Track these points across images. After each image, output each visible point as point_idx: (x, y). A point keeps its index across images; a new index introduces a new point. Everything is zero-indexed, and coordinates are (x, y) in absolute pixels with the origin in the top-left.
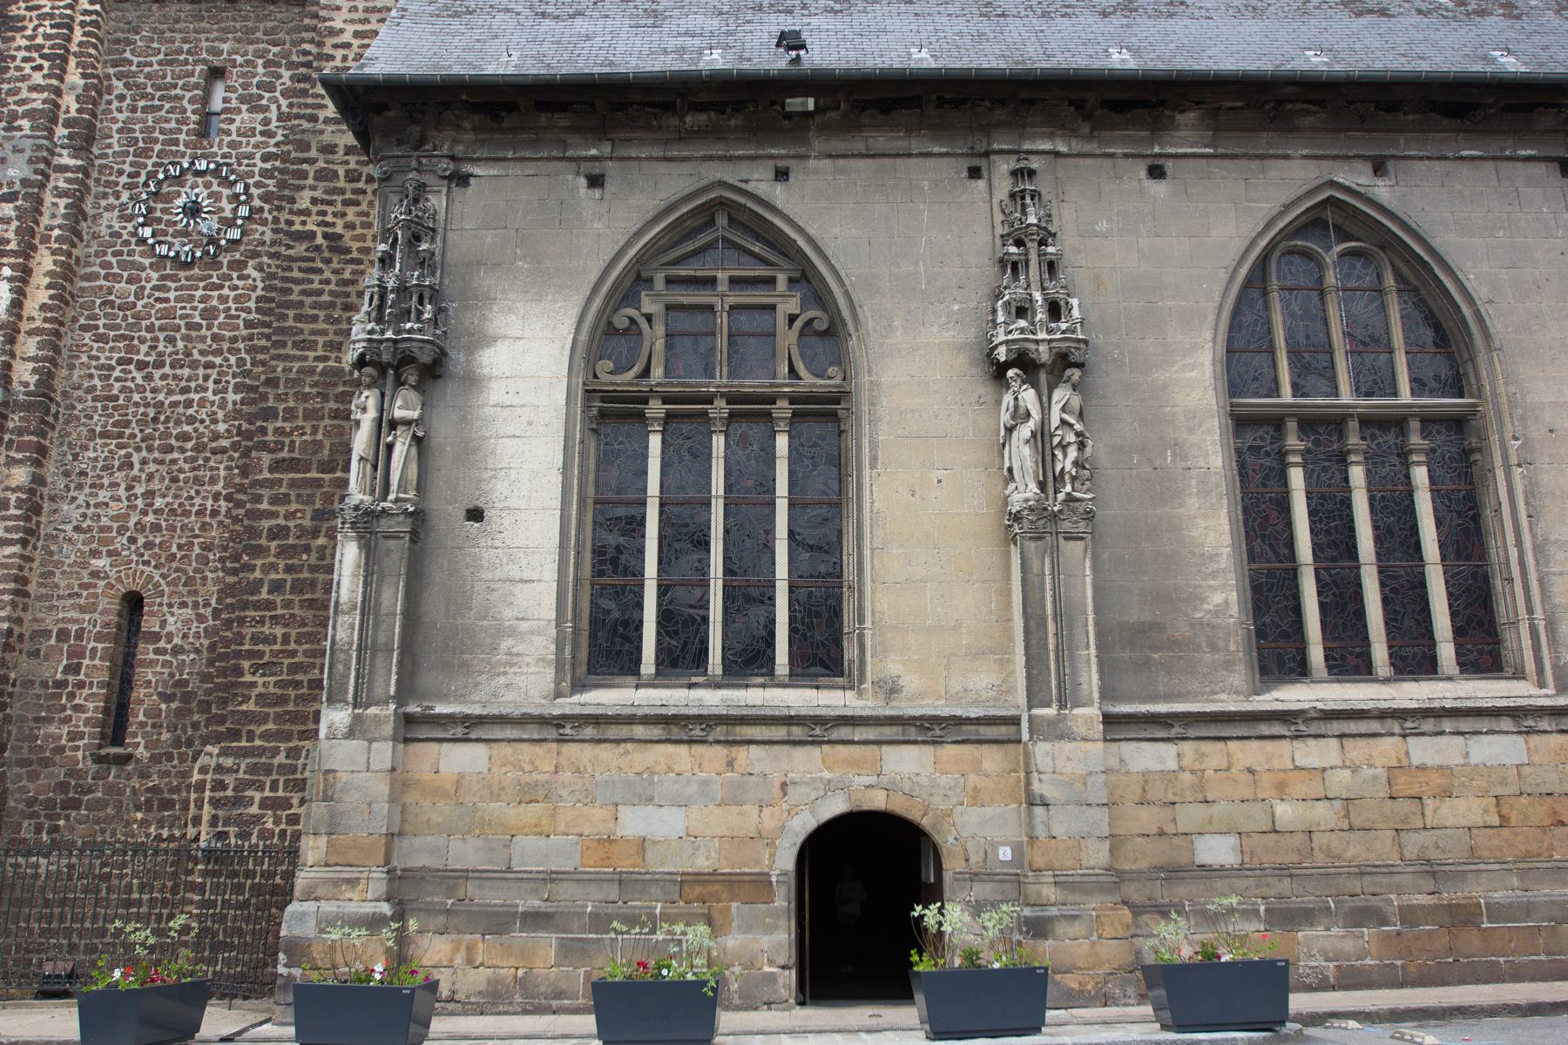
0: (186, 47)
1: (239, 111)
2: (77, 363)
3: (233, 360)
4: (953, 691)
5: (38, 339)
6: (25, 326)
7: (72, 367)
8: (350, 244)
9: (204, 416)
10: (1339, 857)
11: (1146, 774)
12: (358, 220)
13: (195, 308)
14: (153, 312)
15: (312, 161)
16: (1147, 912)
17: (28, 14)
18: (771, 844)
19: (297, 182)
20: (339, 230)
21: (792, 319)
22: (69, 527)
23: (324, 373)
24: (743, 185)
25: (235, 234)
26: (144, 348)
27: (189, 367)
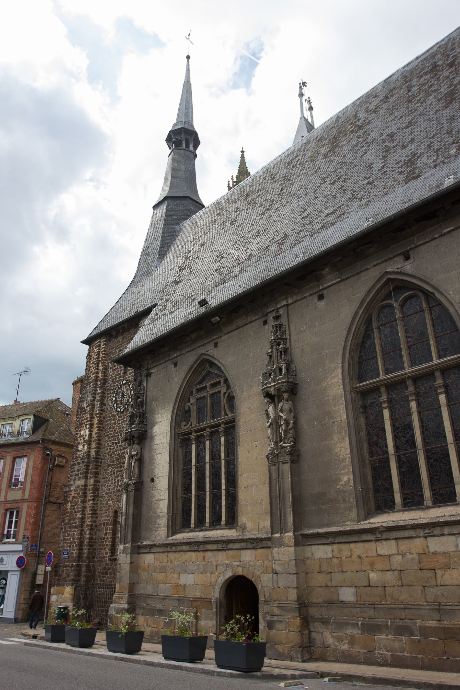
4: (260, 528)
10: (397, 600)
11: (321, 559)
16: (317, 621)
18: (213, 588)
21: (225, 393)
22: (104, 493)
24: (207, 353)
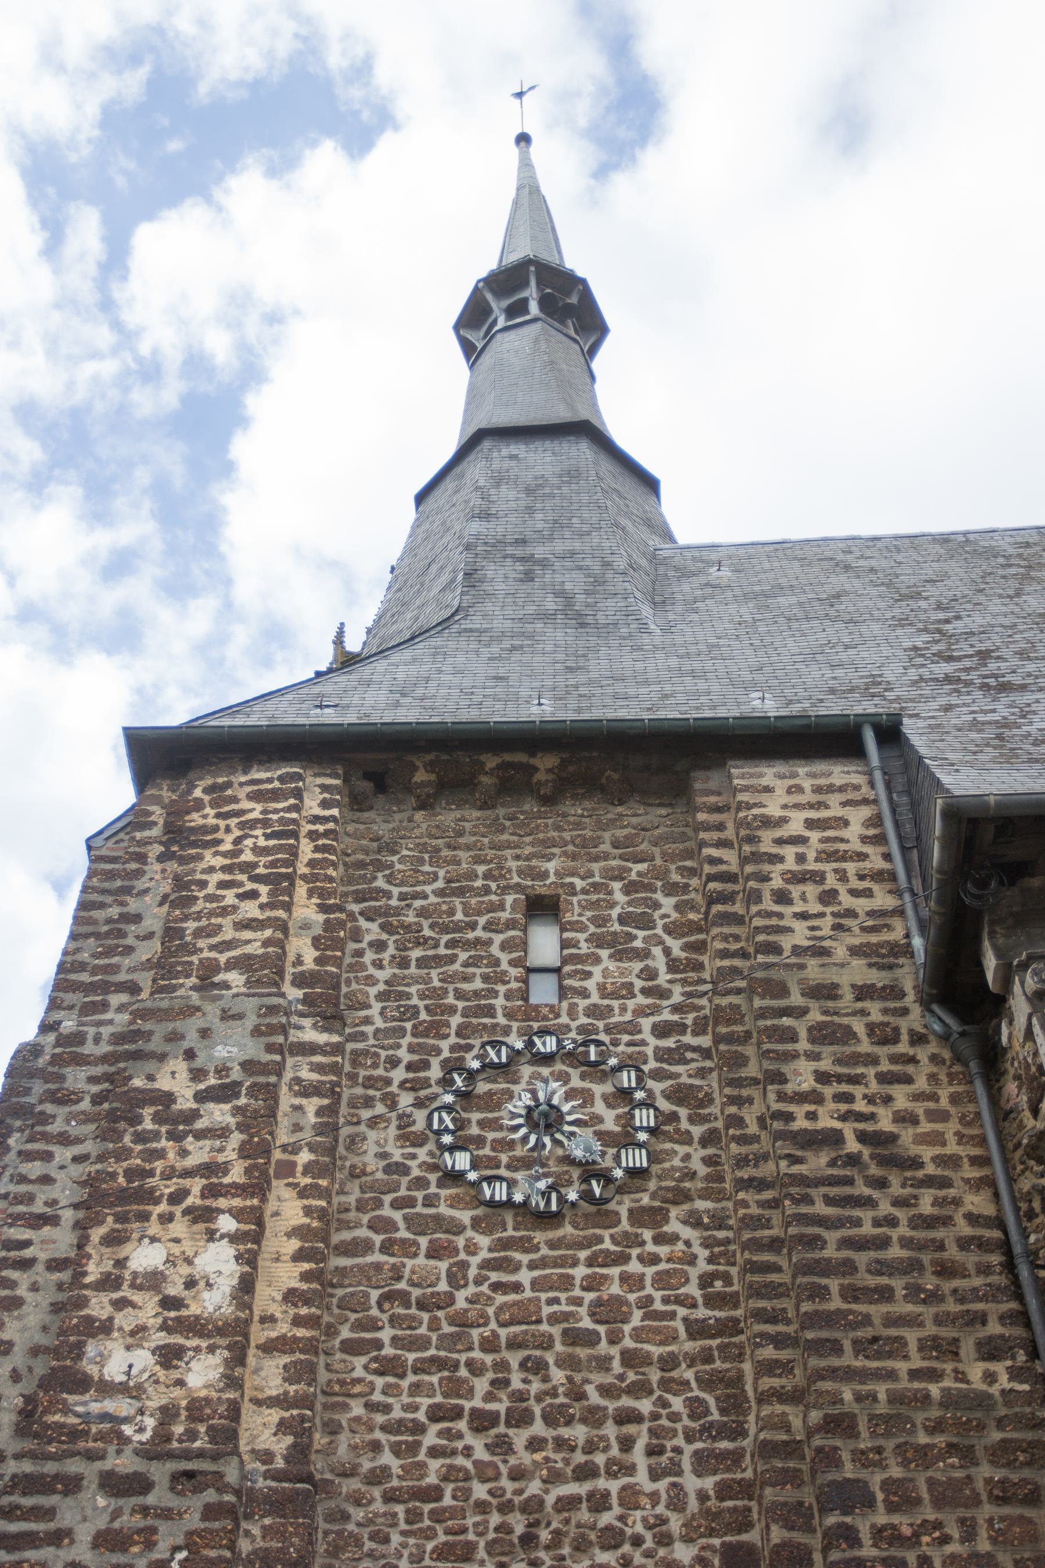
0: (481, 869)
1: (598, 960)
2: (344, 1419)
3: (677, 1404)
5: (286, 1359)
6: (259, 1334)
7: (333, 1429)
8: (915, 1150)
9: (639, 1528)
12: (920, 1109)
13: (578, 1302)
14: (491, 1311)
15: (801, 1012)
17: (222, 823)
19: (780, 1047)
20: (885, 1124)
23: (949, 1400)
25: (638, 1158)
26: (481, 1385)
27: (584, 1421)
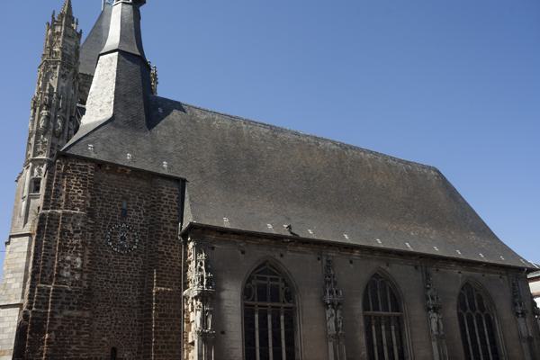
25: (135, 247)
